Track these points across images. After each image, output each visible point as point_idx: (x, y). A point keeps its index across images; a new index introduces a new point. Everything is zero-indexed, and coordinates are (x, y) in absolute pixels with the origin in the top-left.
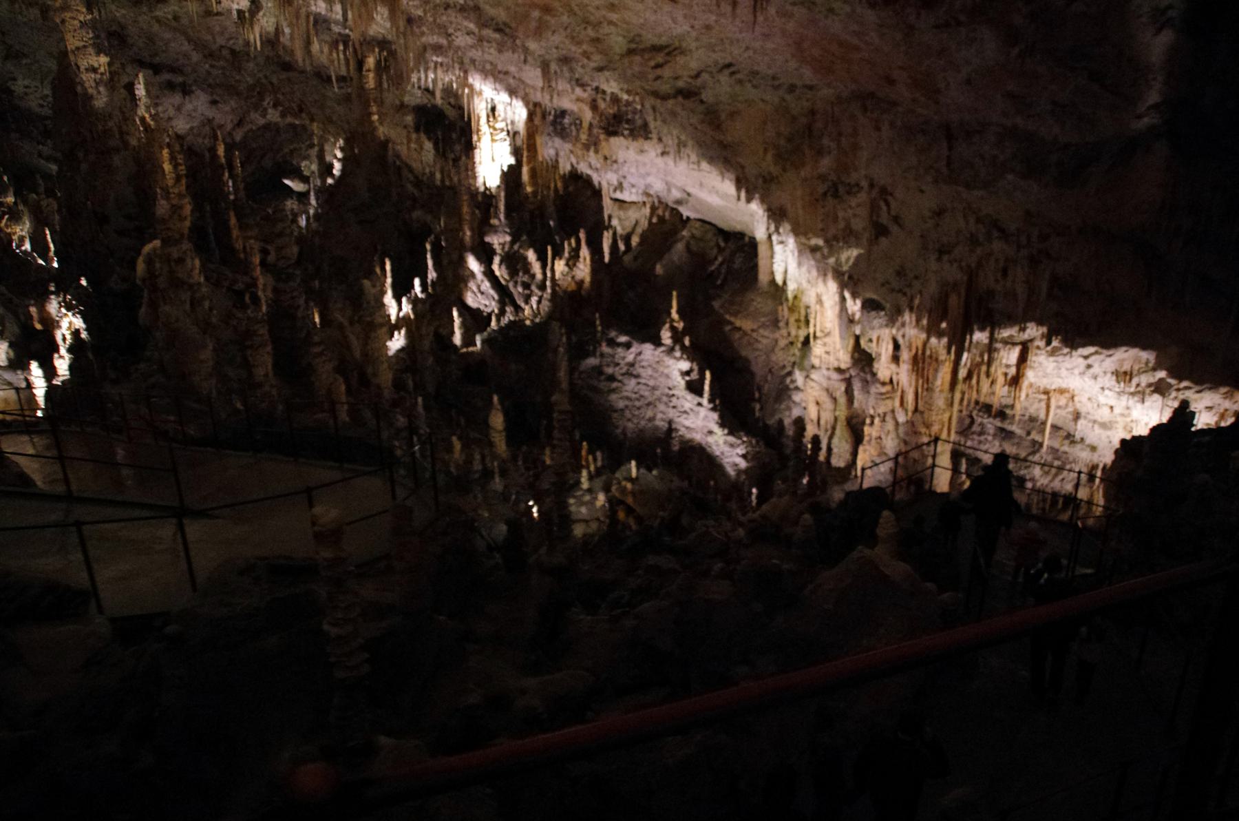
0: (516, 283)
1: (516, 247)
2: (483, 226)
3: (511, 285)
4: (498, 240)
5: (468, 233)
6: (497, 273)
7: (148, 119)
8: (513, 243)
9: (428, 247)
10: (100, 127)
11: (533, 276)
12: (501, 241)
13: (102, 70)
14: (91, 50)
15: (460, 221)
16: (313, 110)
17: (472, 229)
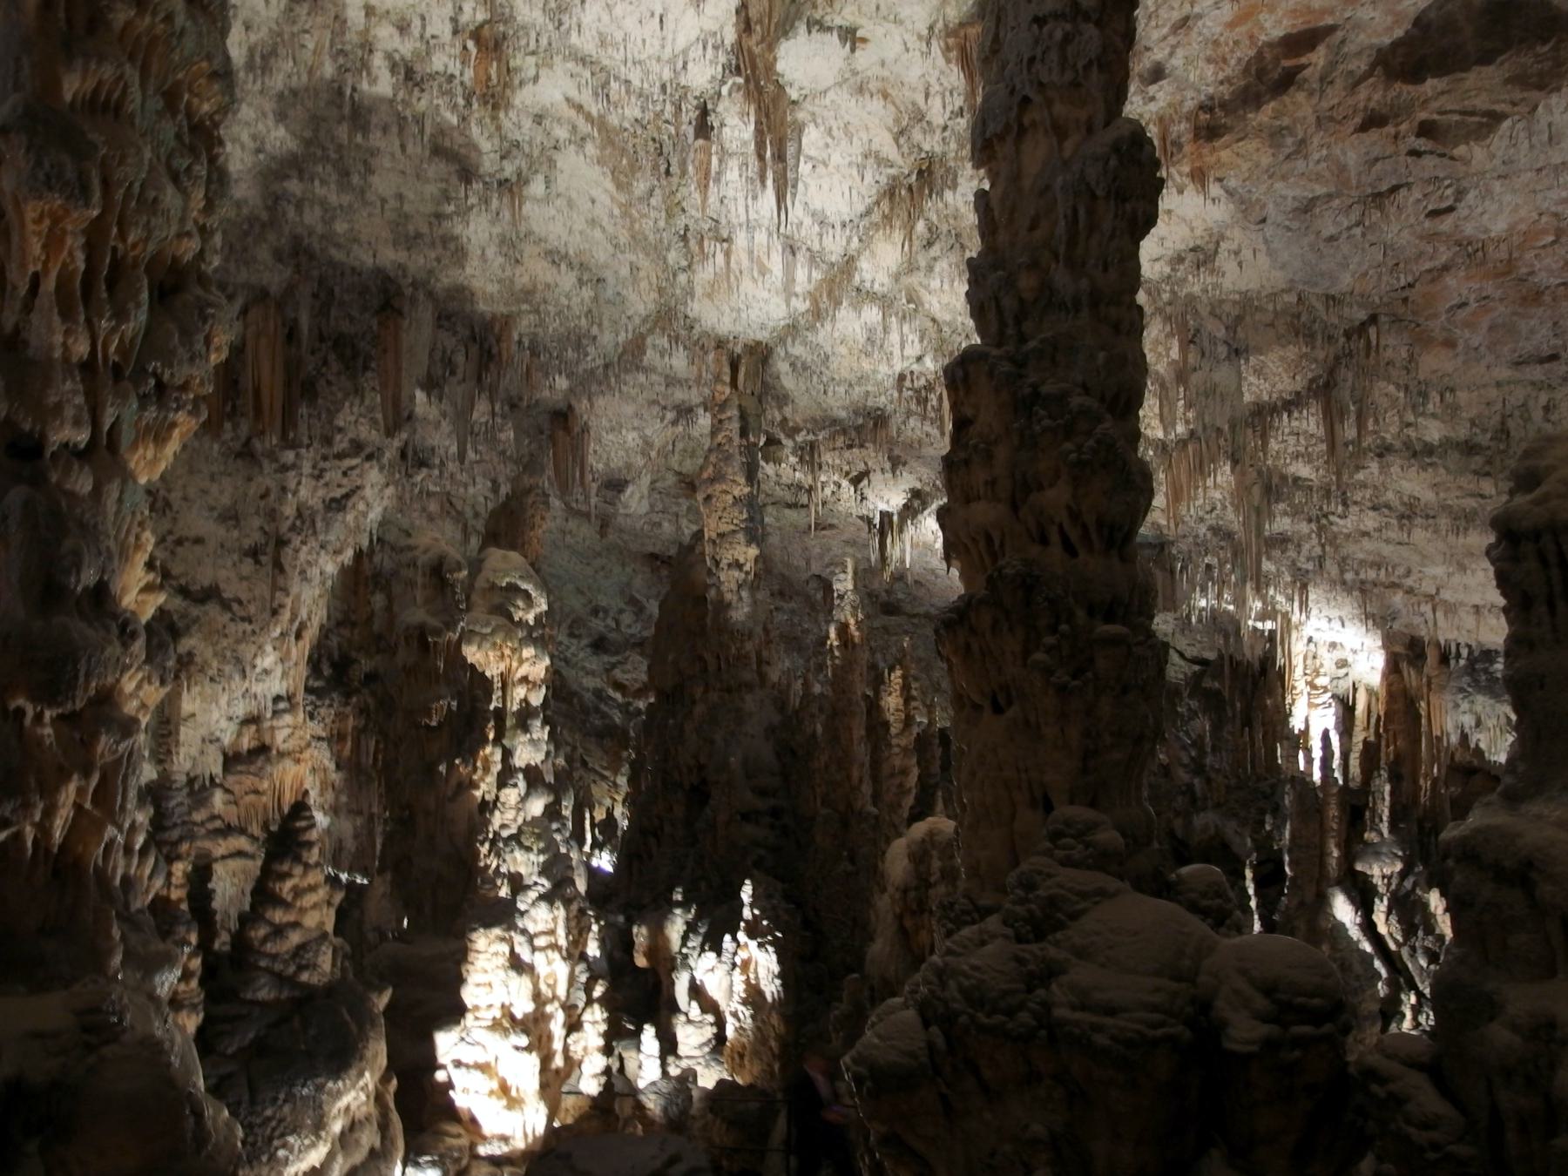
0: (1413, 949)
1: (1408, 884)
2: (1354, 844)
3: (1405, 952)
4: (1381, 871)
5: (1336, 853)
6: (1382, 929)
7: (852, 628)
8: (1403, 875)
10: (733, 650)
11: (1441, 938)
12: (1387, 871)
13: (747, 568)
14: (741, 537)
15: (1323, 830)
17: (1338, 846)
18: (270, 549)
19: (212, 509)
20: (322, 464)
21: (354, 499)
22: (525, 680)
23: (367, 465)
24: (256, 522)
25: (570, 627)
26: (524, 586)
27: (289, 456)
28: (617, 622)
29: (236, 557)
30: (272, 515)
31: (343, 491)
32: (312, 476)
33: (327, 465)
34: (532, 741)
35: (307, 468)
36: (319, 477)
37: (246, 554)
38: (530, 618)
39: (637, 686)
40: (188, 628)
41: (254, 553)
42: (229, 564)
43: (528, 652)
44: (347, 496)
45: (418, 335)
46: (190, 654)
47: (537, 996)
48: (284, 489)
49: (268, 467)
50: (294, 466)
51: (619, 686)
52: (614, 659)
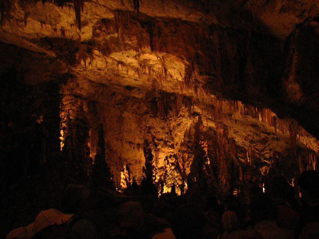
9: (293, 180)
16: (309, 145)
18: (169, 132)
19: (160, 127)
20: (176, 119)
21: (181, 124)
22: (171, 152)
23: (183, 118)
24: (167, 129)
25: (245, 138)
26: (169, 140)
27: (170, 118)
28: (254, 137)
29: (165, 134)
30: (169, 127)
31: (180, 122)
32: (174, 121)
33: (176, 119)
34: (171, 159)
35: (173, 120)
36: (176, 121)
37: (166, 133)
38: (170, 144)
39: (261, 149)
40: (158, 145)
41: (167, 133)
42: (164, 135)
43: (170, 148)
44: (180, 123)
45: (179, 101)
46: (159, 148)
47: (126, 177)
48: (170, 123)
49: (168, 120)
50: (171, 120)
51: (257, 150)
52: (255, 144)
